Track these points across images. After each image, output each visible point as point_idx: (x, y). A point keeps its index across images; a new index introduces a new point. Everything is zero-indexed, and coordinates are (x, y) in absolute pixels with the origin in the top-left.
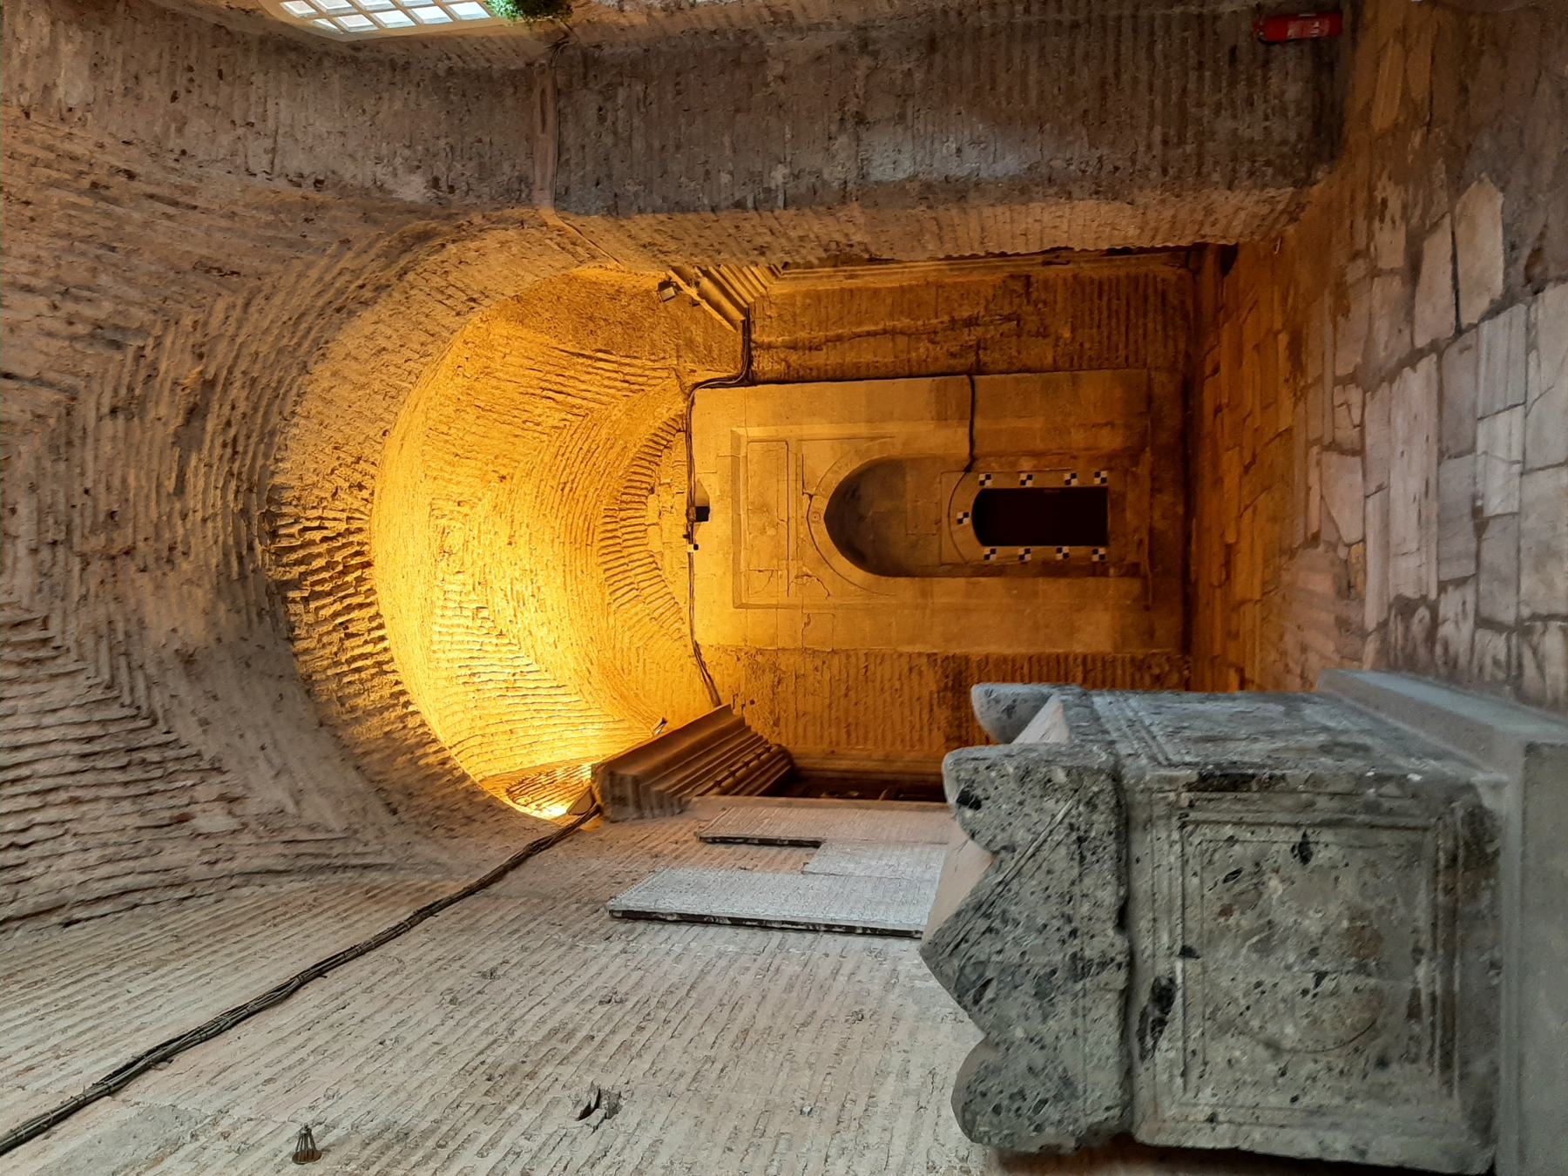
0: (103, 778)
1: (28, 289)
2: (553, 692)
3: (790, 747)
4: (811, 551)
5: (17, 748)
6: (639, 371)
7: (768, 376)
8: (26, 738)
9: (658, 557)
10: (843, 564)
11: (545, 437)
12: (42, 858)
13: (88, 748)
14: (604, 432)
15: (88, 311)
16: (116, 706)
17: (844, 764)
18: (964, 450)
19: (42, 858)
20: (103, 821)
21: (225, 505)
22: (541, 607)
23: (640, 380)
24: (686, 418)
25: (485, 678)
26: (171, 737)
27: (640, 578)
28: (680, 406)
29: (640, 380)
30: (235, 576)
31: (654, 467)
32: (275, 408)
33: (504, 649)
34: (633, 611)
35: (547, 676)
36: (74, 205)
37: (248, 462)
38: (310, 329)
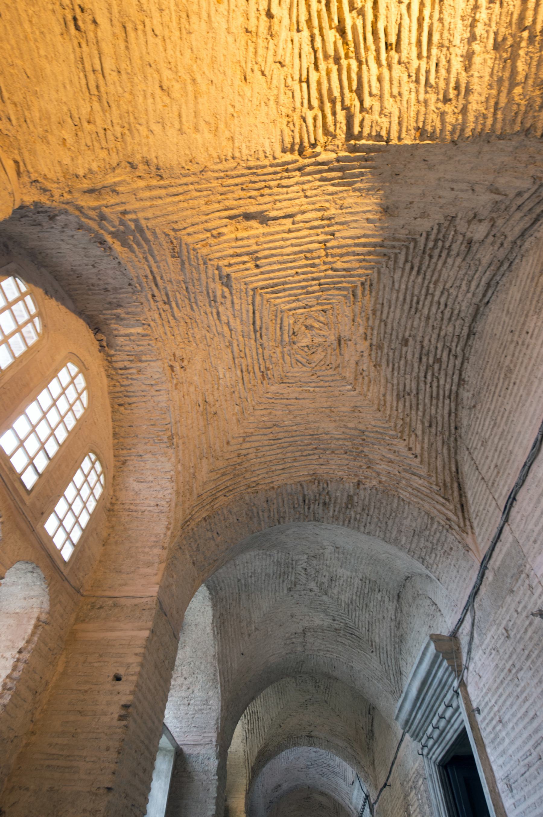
0: (432, 267)
1: (218, 313)
5: (405, 299)
8: (401, 298)
12: (454, 303)
13: (416, 269)
15: (219, 293)
16: (399, 255)
19: (454, 303)
20: (451, 274)
21: (297, 184)
26: (424, 235)
36: (177, 306)
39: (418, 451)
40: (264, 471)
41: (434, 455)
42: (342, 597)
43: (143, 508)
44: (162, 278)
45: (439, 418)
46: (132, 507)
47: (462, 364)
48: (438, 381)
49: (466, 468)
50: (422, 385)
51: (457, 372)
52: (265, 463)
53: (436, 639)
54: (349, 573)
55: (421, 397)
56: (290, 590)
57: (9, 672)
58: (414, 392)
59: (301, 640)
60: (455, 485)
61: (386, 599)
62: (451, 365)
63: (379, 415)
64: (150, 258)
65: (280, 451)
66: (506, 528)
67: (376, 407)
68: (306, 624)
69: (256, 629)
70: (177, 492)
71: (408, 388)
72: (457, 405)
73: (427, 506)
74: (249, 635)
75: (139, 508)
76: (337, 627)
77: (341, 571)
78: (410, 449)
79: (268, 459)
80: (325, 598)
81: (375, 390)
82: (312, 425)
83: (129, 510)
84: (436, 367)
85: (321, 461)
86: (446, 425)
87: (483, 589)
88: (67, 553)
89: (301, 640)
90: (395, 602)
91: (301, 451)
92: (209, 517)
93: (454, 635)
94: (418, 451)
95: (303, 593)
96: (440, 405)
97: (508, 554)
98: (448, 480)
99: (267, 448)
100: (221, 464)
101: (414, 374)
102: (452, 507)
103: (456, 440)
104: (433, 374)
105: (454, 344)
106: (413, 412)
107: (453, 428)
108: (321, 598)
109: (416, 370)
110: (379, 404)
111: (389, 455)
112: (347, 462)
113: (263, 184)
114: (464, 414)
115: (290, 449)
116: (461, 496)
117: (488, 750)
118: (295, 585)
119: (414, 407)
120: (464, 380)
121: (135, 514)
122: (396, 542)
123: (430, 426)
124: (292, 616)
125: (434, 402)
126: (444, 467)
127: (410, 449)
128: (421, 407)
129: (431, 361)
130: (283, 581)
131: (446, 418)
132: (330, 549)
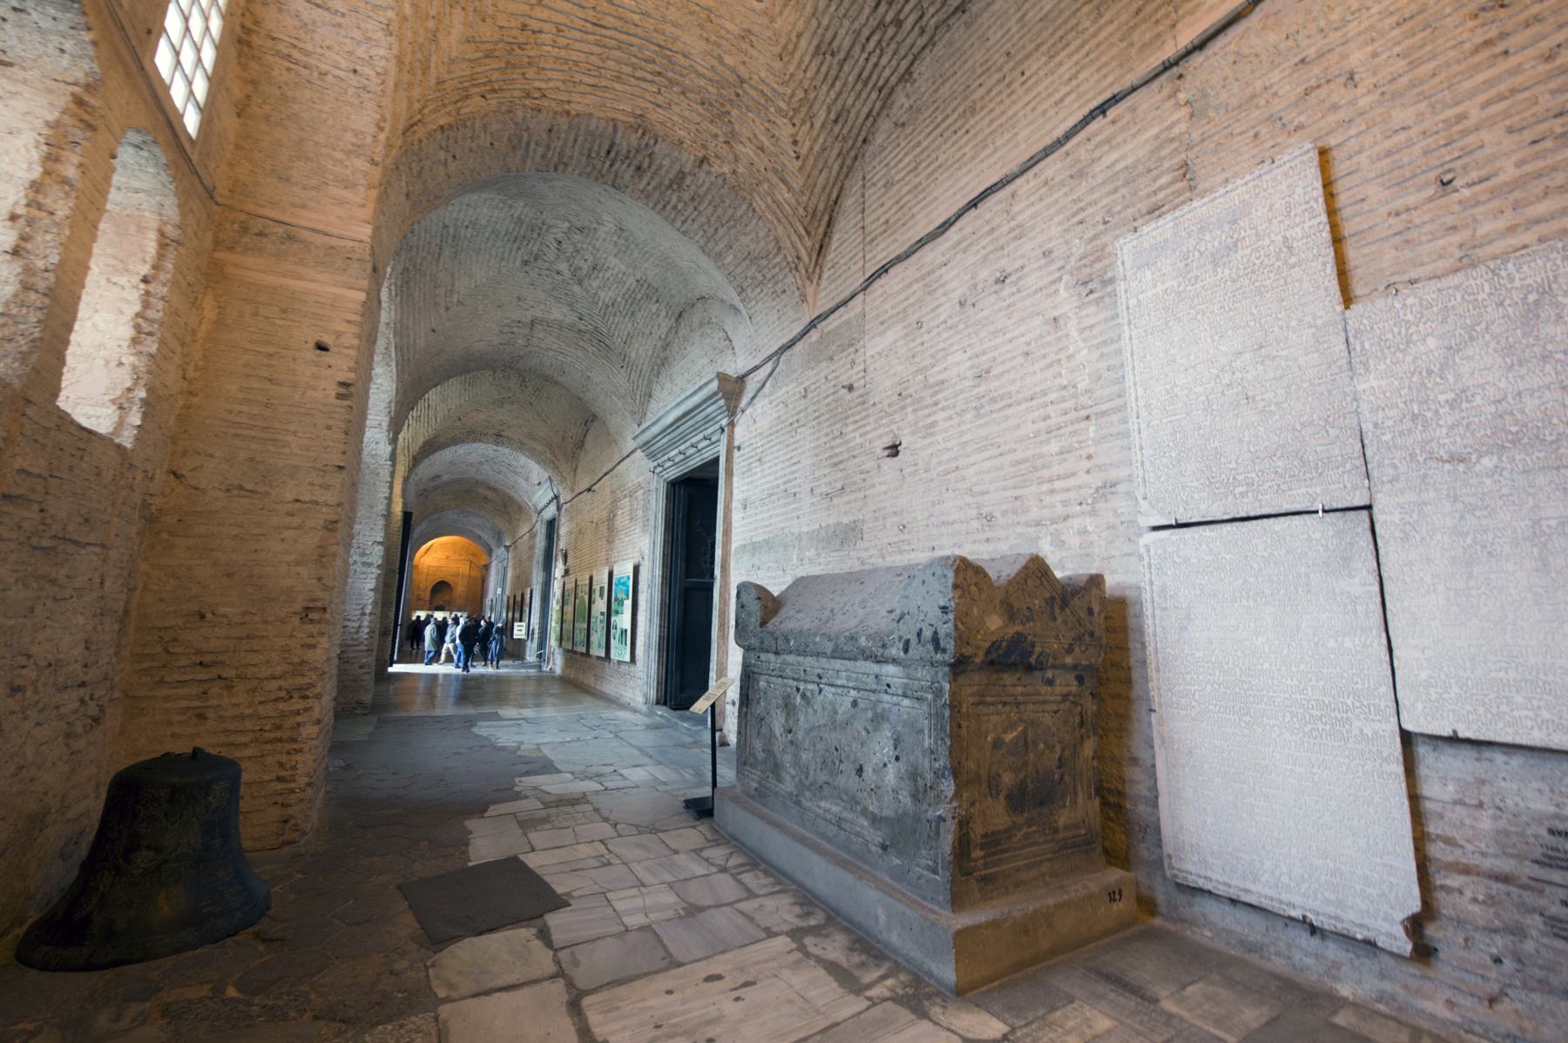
39: (803, 151)
40: (560, 76)
41: (820, 165)
42: (602, 295)
43: (324, 67)
45: (852, 115)
46: (296, 54)
47: (923, 48)
48: (880, 57)
49: (849, 202)
50: (857, 49)
51: (910, 57)
52: (566, 61)
53: (722, 377)
54: (623, 267)
55: (846, 68)
56: (526, 263)
57: (138, 308)
58: (842, 55)
59: (526, 331)
60: (826, 218)
61: (663, 314)
62: (909, 41)
63: (778, 65)
65: (597, 50)
66: (860, 297)
67: (778, 49)
68: (539, 314)
69: (460, 302)
70: (400, 62)
71: (836, 43)
72: (883, 107)
73: (780, 231)
74: (448, 308)
75: (312, 61)
76: (583, 328)
77: (613, 261)
78: (795, 143)
79: (574, 56)
80: (576, 289)
81: (791, 19)
82: (669, 29)
83: (288, 57)
84: (891, 31)
85: (660, 100)
86: (855, 131)
87: (799, 346)
88: (192, 122)
89: (526, 331)
90: (673, 320)
91: (633, 66)
92: (451, 126)
93: (742, 379)
94: (803, 151)
95: (544, 272)
96: (864, 95)
97: (848, 323)
98: (821, 207)
99: (578, 35)
100: (487, 32)
101: (856, 25)
102: (809, 244)
103: (856, 157)
104: (880, 41)
105: (932, 10)
106: (825, 88)
107: (861, 139)
108: (569, 287)
109: (862, 19)
110: (785, 47)
111: (763, 139)
112: (699, 119)
114: (885, 125)
115: (617, 53)
116: (825, 234)
117: (735, 479)
118: (536, 259)
119: (830, 81)
120: (910, 74)
121: (304, 72)
122: (718, 257)
123: (836, 121)
124: (519, 299)
125: (859, 86)
126: (824, 188)
127: (795, 143)
128: (838, 84)
129: (888, 19)
130: (519, 249)
131: (860, 121)
132: (611, 227)
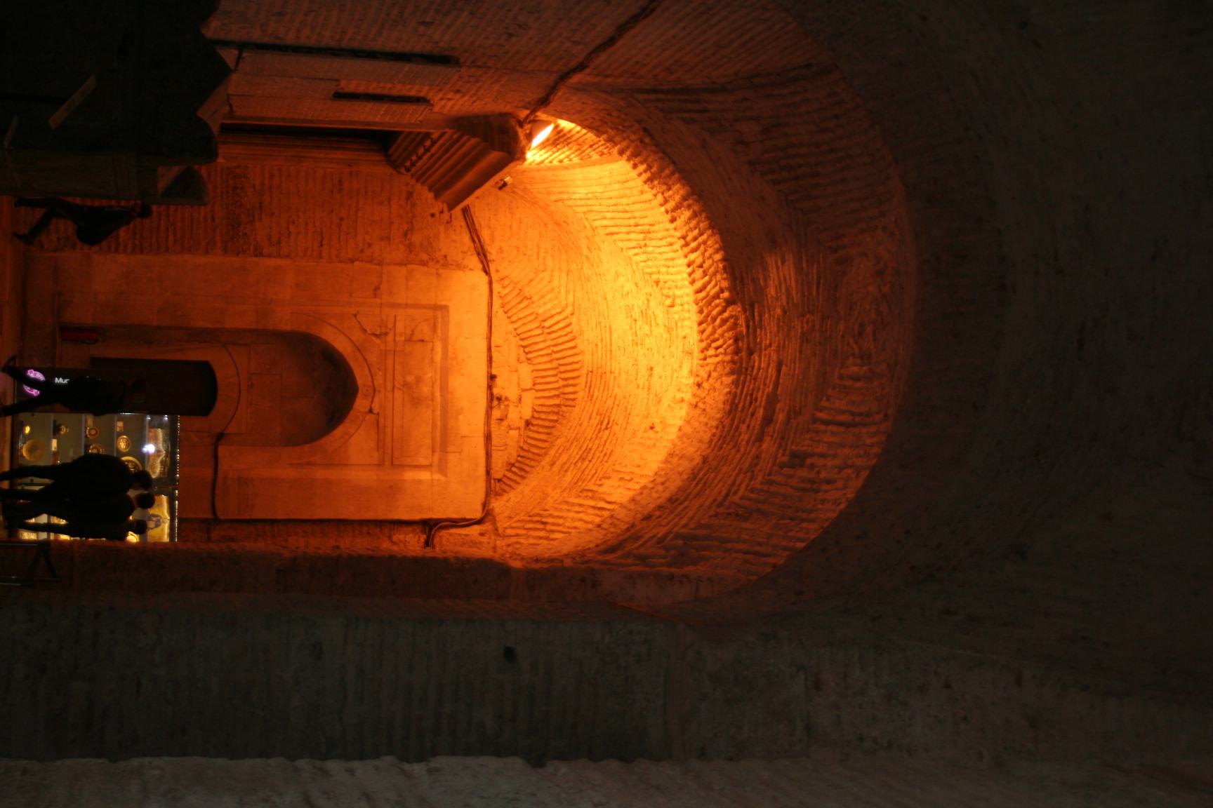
2: (615, 229)
3: (389, 170)
4: (373, 358)
6: (532, 533)
7: (409, 529)
9: (523, 357)
10: (342, 345)
11: (617, 468)
14: (569, 477)
17: (339, 155)
18: (222, 451)
22: (629, 309)
23: (531, 525)
24: (489, 493)
25: (664, 242)
27: (541, 338)
28: (497, 505)
29: (531, 525)
30: (756, 306)
31: (526, 447)
32: (726, 430)
33: (654, 269)
34: (549, 306)
35: (621, 244)
37: (745, 389)
38: (697, 484)
44: (760, 544)
64: (729, 545)
113: (749, 398)
